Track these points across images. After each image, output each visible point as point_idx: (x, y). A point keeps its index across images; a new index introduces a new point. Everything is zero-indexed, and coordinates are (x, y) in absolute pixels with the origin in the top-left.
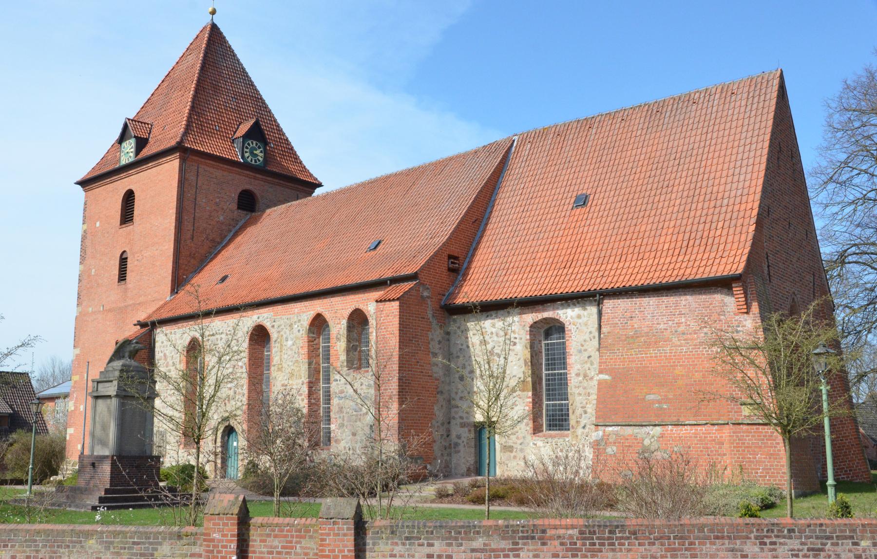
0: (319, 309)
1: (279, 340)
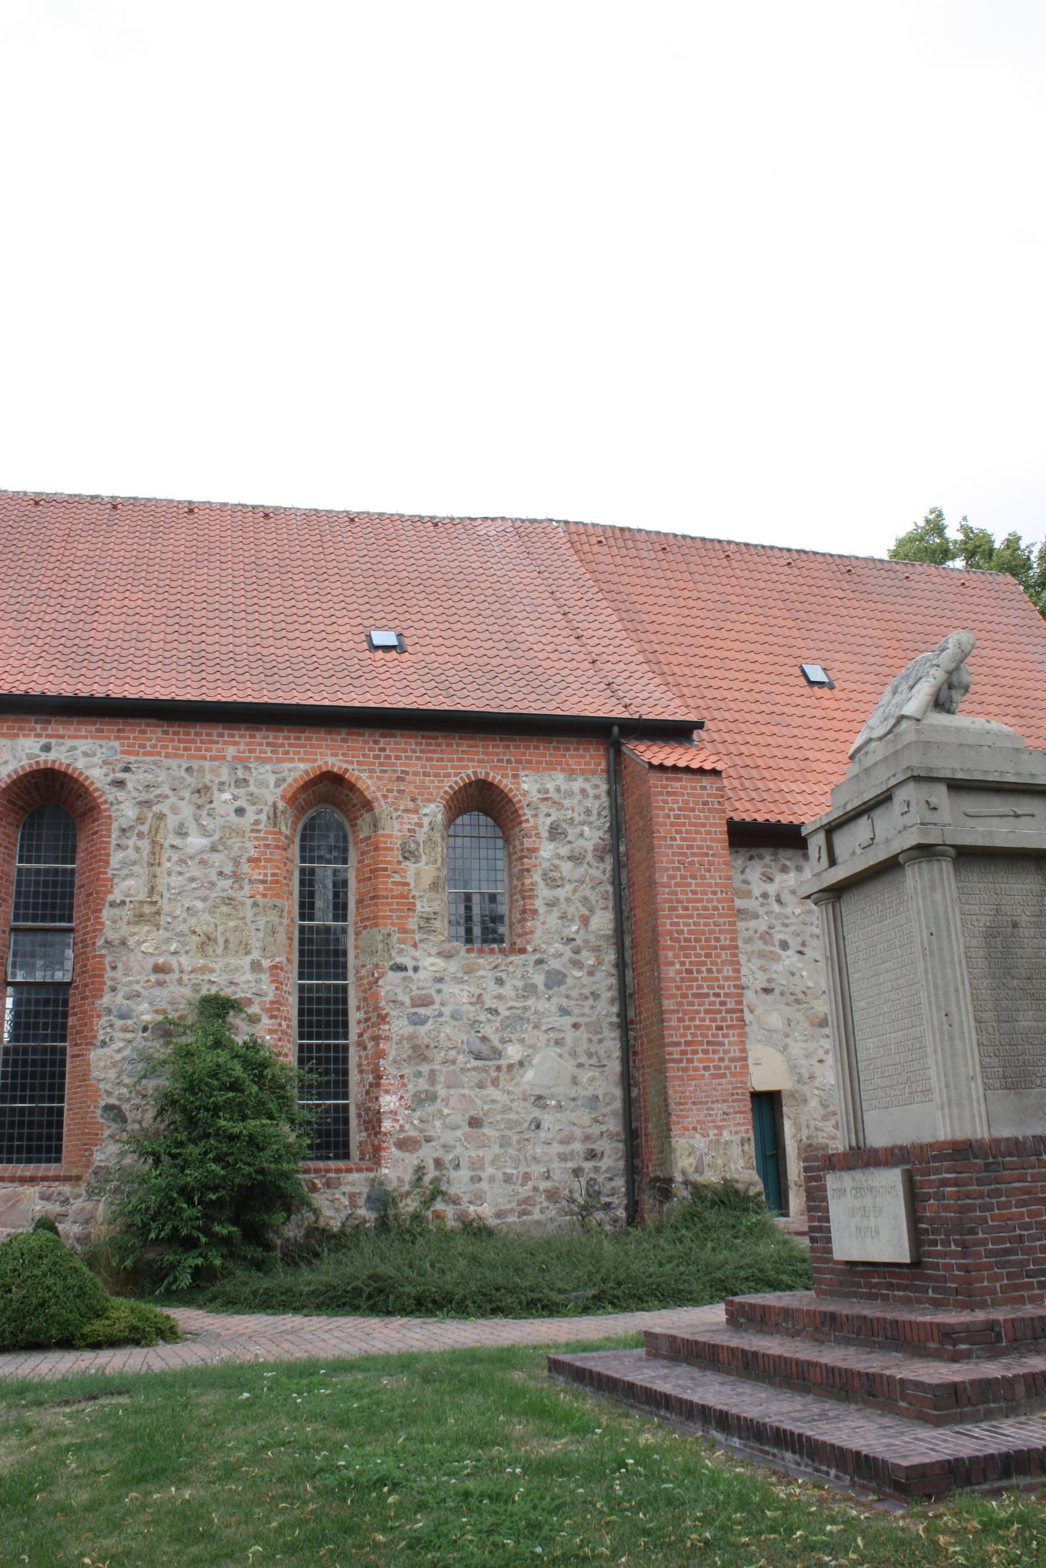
0: (331, 760)
1: (145, 828)
